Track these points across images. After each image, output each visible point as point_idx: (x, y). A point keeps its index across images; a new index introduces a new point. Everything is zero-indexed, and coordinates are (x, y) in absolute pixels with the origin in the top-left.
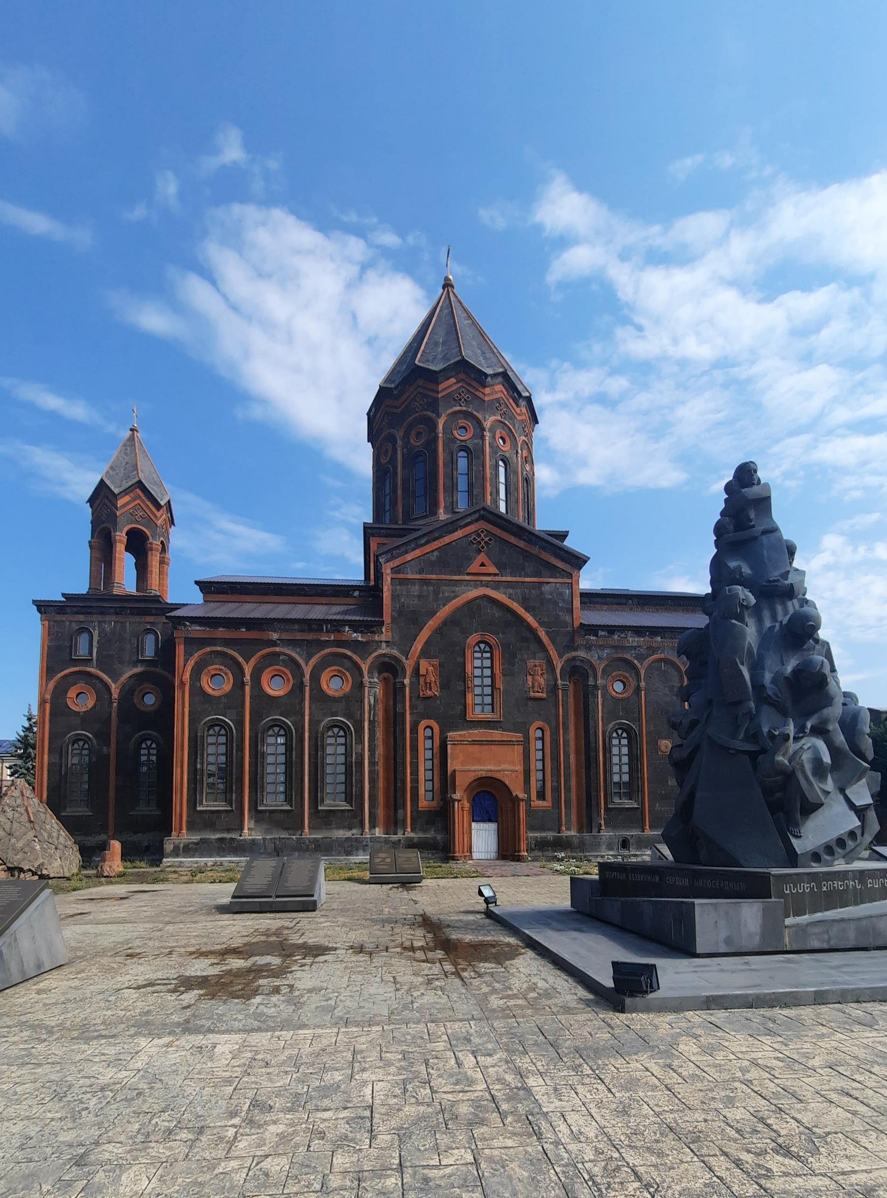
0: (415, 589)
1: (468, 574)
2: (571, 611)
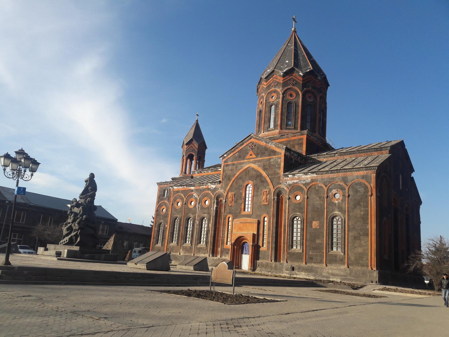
1: (247, 159)
2: (280, 168)
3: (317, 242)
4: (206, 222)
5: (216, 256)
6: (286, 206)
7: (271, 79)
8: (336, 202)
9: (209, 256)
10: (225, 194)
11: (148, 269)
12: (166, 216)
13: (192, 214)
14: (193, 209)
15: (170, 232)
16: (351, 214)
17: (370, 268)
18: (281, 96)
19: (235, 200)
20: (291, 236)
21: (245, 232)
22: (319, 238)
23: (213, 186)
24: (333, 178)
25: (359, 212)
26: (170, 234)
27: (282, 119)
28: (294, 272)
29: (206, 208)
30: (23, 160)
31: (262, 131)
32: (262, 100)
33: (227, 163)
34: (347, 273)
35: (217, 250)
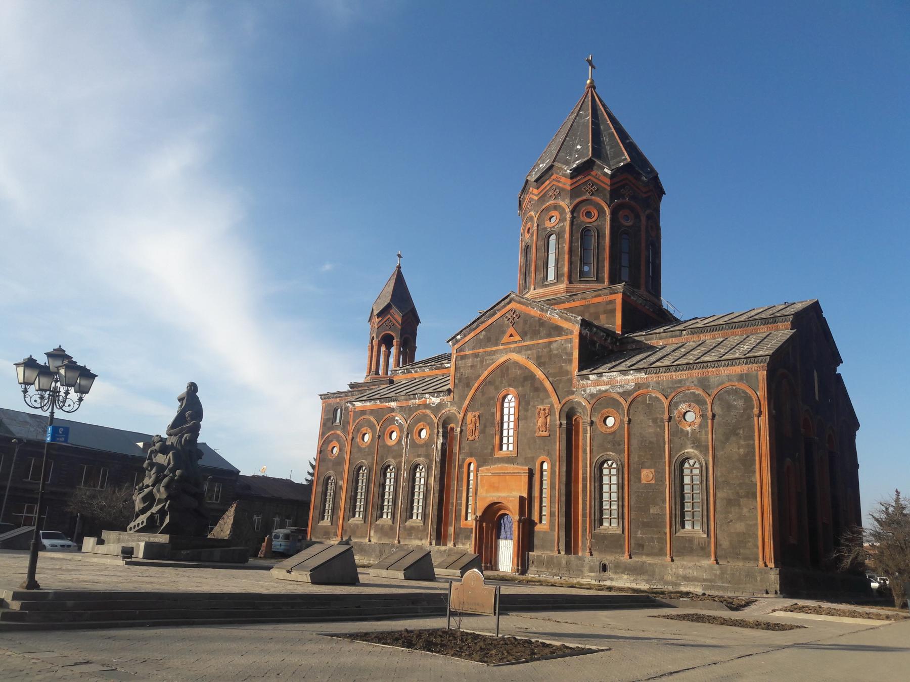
0: (469, 362)
1: (503, 344)
2: (570, 361)
3: (652, 511)
4: (423, 474)
5: (445, 544)
6: (585, 438)
7: (548, 182)
8: (689, 429)
9: (431, 544)
10: (460, 417)
11: (314, 583)
12: (339, 462)
13: (394, 458)
14: (396, 448)
15: (349, 495)
16: (719, 454)
17: (761, 563)
18: (568, 216)
19: (482, 427)
20: (597, 501)
21: (503, 494)
22: (655, 504)
23: (436, 400)
24: (680, 381)
25: (735, 449)
26: (348, 500)
27: (571, 263)
28: (606, 574)
29: (421, 446)
30: (62, 371)
31: (532, 287)
32: (529, 225)
33: (462, 353)
34: (716, 575)
35: (446, 531)
